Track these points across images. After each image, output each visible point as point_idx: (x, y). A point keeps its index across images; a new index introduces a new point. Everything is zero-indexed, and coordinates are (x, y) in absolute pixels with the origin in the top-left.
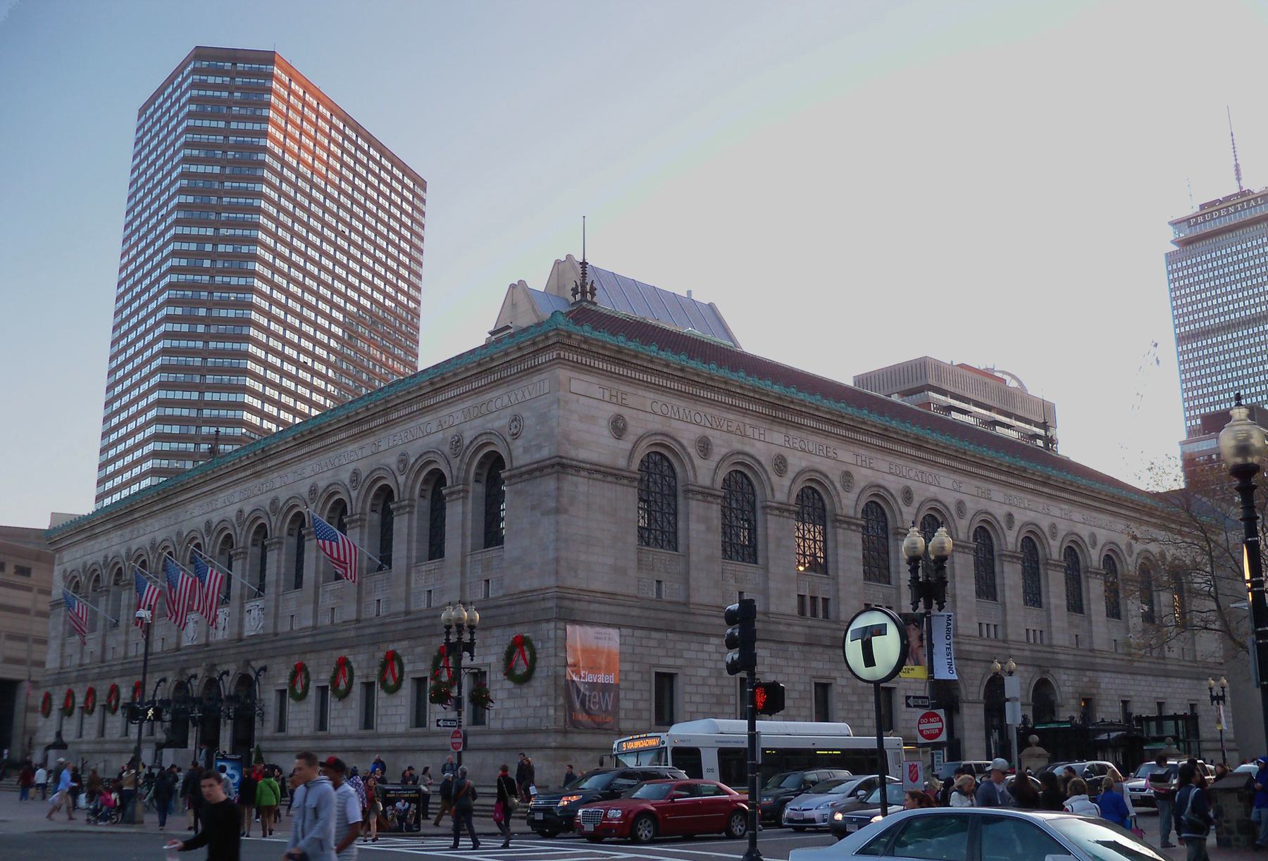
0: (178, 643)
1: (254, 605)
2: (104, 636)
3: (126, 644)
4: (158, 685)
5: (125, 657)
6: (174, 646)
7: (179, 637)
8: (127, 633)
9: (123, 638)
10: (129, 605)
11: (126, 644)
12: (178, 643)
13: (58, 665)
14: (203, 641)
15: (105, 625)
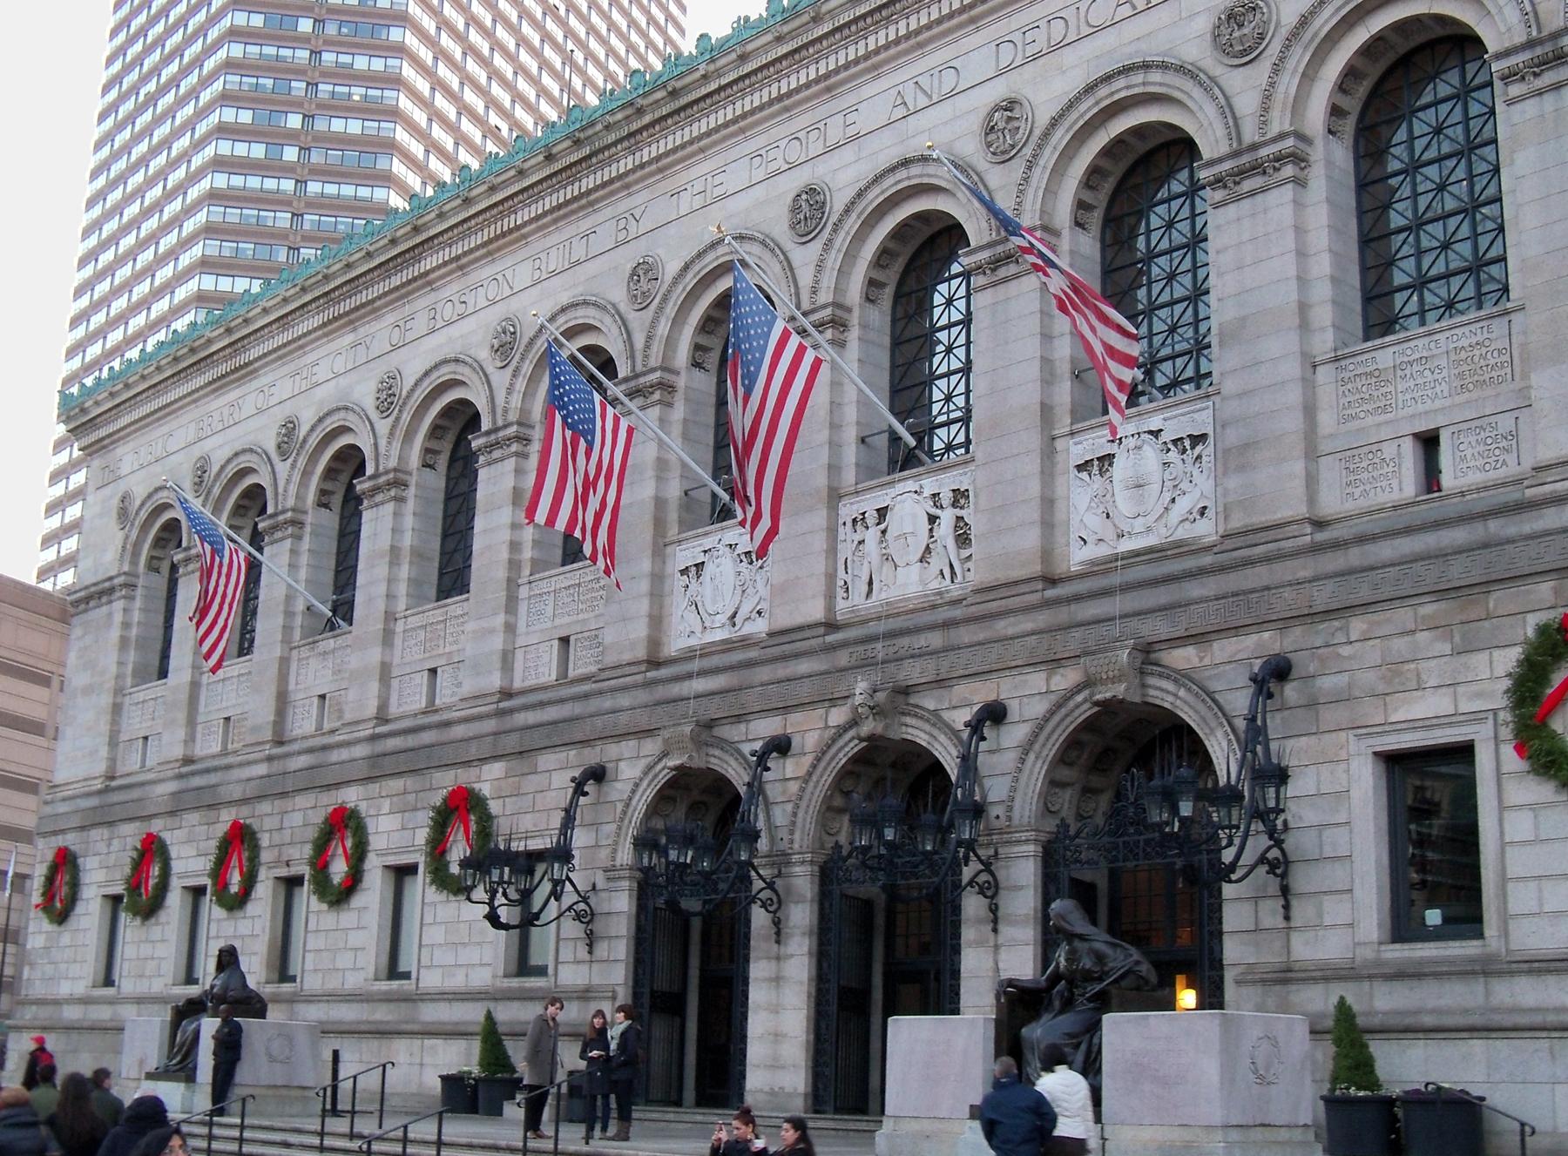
0: (654, 643)
1: (909, 499)
2: (284, 662)
3: (385, 673)
4: (579, 791)
5: (382, 718)
6: (641, 653)
7: (657, 621)
8: (387, 638)
9: (375, 655)
10: (394, 551)
11: (385, 673)
12: (654, 643)
13: (101, 768)
14: (815, 611)
15: (287, 629)
